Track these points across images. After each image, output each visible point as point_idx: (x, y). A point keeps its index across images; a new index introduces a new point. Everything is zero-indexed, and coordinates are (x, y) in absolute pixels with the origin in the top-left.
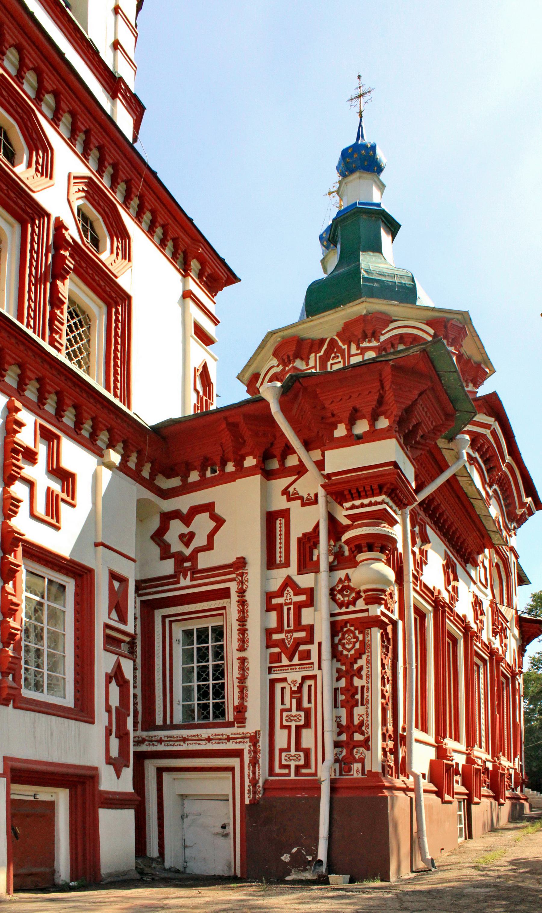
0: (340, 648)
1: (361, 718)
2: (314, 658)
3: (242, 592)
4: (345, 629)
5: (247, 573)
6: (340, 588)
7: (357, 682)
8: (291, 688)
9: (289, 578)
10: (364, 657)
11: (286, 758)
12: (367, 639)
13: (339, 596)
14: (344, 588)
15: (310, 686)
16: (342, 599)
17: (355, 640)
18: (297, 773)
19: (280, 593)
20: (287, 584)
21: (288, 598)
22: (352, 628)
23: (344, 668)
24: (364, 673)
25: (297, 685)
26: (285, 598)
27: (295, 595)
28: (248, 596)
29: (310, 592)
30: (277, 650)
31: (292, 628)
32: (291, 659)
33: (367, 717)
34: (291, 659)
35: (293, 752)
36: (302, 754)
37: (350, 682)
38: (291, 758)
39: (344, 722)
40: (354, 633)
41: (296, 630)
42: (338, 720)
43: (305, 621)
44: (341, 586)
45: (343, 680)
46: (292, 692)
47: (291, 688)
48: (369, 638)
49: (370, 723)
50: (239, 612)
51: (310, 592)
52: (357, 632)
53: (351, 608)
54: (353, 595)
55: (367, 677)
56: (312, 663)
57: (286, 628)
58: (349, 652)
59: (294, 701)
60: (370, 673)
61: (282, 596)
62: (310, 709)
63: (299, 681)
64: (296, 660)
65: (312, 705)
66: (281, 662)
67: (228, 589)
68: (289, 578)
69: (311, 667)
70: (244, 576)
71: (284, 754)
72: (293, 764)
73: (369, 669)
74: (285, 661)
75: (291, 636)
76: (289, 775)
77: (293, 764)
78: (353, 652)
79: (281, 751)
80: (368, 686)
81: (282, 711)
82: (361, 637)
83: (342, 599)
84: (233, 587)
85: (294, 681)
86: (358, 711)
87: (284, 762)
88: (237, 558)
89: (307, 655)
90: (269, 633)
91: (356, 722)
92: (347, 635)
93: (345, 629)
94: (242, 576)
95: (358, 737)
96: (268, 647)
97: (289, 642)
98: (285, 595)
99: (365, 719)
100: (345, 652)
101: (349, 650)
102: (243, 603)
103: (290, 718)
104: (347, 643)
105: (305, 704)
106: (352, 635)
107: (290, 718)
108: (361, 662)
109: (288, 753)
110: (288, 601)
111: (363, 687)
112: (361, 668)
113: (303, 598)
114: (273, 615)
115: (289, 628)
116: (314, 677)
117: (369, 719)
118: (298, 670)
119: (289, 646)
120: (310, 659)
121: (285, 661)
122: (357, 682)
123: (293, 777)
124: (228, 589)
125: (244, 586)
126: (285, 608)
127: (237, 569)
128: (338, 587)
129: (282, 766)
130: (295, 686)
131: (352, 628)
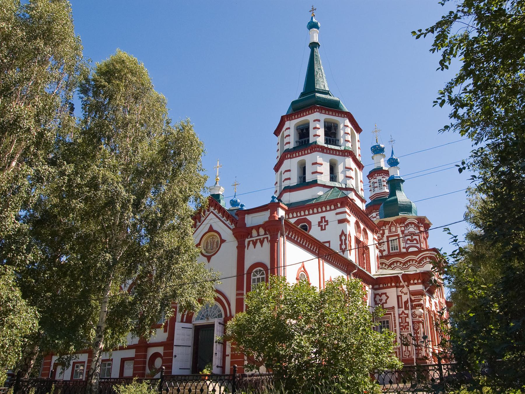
3: (394, 314)
29: (407, 314)
43: (407, 321)
51: (407, 314)
84: (392, 313)
89: (408, 329)
90: (400, 323)
102: (394, 316)
108: (419, 331)
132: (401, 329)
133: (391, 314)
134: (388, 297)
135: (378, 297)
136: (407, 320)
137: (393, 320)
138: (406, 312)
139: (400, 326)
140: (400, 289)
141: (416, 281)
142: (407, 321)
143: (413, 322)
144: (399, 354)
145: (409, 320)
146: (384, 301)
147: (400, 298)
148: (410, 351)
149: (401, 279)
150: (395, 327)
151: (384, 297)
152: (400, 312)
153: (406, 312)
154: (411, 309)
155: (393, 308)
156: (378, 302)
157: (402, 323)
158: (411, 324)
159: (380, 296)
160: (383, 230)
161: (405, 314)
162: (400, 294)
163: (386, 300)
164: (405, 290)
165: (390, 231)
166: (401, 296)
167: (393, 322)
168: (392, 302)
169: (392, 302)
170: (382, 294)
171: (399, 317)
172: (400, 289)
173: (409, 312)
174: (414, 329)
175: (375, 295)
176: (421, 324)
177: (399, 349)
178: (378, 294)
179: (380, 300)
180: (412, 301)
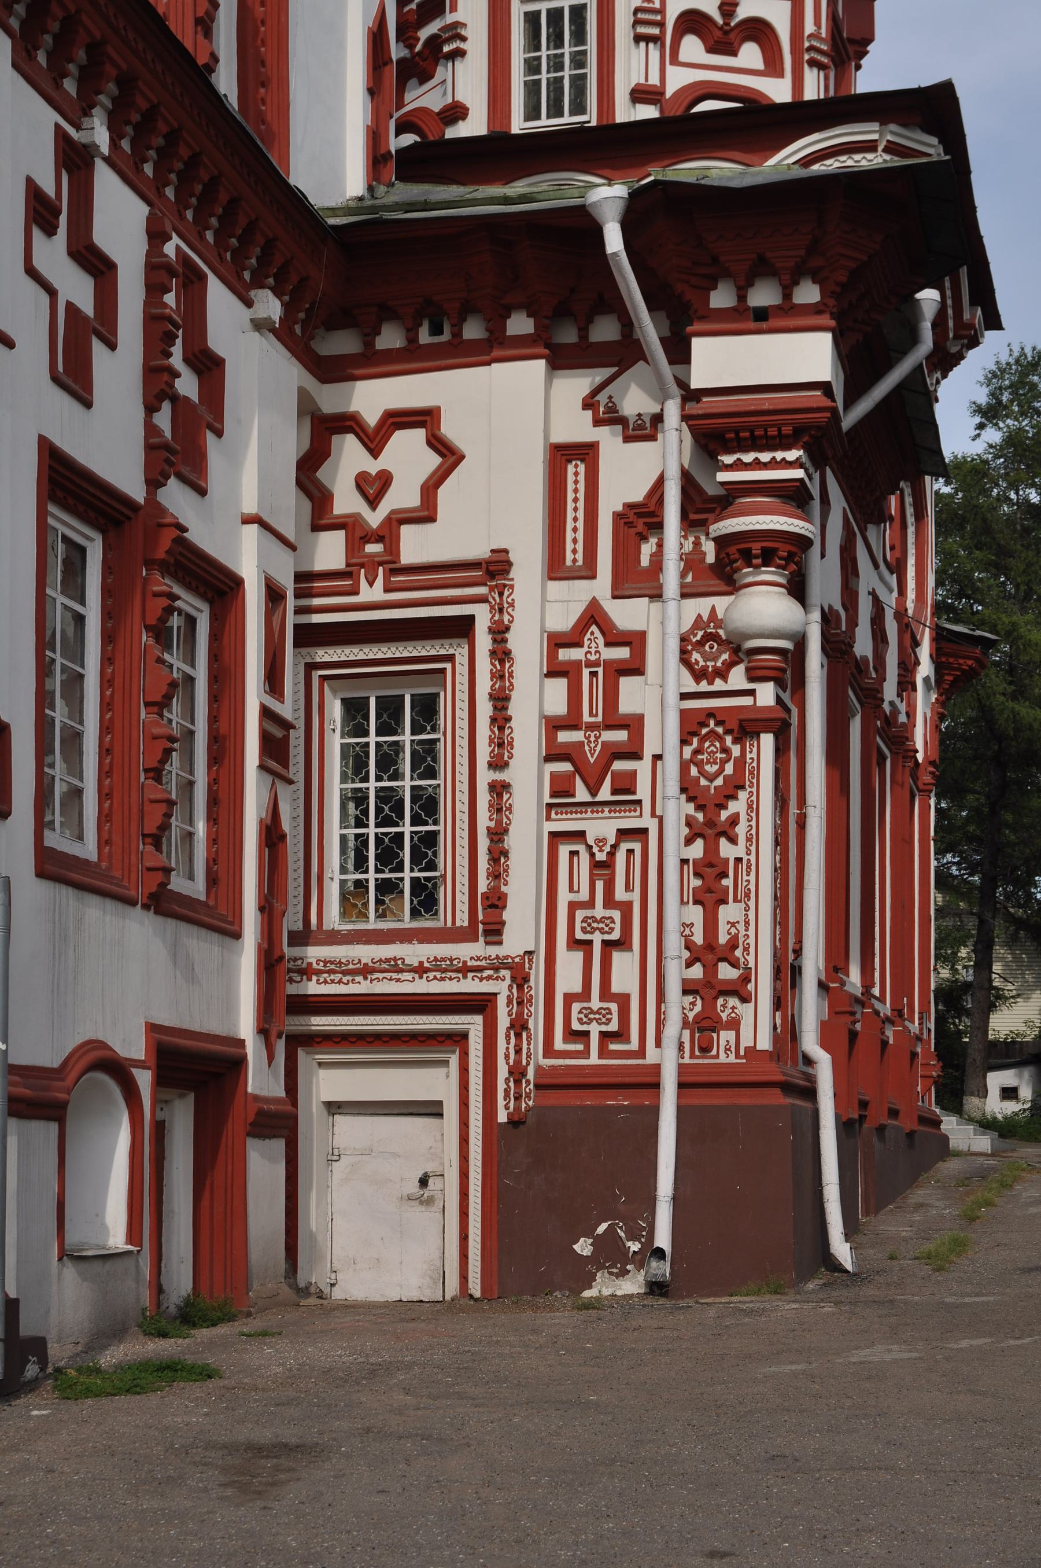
0: (694, 771)
1: (733, 931)
2: (643, 791)
3: (499, 632)
4: (704, 731)
5: (512, 587)
6: (698, 637)
7: (726, 850)
8: (592, 855)
9: (594, 604)
10: (742, 795)
11: (582, 1016)
12: (749, 756)
13: (696, 656)
14: (708, 637)
15: (630, 851)
16: (702, 663)
17: (724, 756)
18: (603, 1053)
19: (573, 639)
20: (592, 616)
21: (593, 650)
22: (720, 730)
23: (700, 816)
24: (741, 830)
25: (607, 849)
26: (586, 649)
27: (608, 644)
28: (514, 641)
29: (636, 641)
30: (566, 767)
31: (600, 718)
32: (594, 791)
33: (747, 930)
34: (594, 791)
35: (595, 1003)
36: (614, 1007)
37: (712, 849)
38: (591, 1016)
39: (698, 939)
40: (721, 740)
41: (609, 727)
42: (687, 932)
43: (626, 706)
44: (700, 633)
45: (699, 843)
46: (595, 865)
47: (592, 855)
48: (754, 755)
49: (752, 941)
50: (493, 676)
51: (636, 641)
52: (729, 739)
53: (719, 685)
54: (725, 656)
55: (749, 840)
56: (639, 802)
57: (586, 718)
58: (711, 781)
59: (600, 885)
60: (753, 832)
61: (579, 644)
62: (629, 904)
63: (612, 840)
64: (605, 793)
65: (635, 897)
66: (573, 795)
67: (471, 619)
68: (594, 604)
69: (635, 811)
70: (506, 593)
71: (576, 1007)
72: (595, 1029)
73: (754, 823)
74: (582, 794)
75: (597, 738)
76: (586, 1053)
77: (595, 1029)
78: (719, 781)
79: (570, 999)
80: (749, 860)
81: (573, 906)
82: (736, 751)
83: (702, 663)
85: (601, 841)
86: (729, 913)
87: (576, 1026)
88: (492, 551)
89: (625, 785)
90: (553, 725)
91: (723, 939)
92: (707, 744)
93: (704, 731)
94: (501, 594)
95: (726, 972)
96: (549, 758)
97: (592, 751)
98: (586, 643)
99: (743, 932)
100: (703, 782)
101: (711, 779)
102: (501, 654)
103: (589, 925)
104: (708, 762)
105: (620, 894)
106: (718, 744)
107: (589, 925)
108: (737, 806)
109: (585, 1005)
110: (593, 658)
111: (739, 860)
112: (734, 820)
113: (622, 653)
114: (559, 686)
115: (593, 720)
116: (641, 833)
117: (751, 932)
118: (606, 814)
119: (592, 760)
120: (634, 793)
121: (582, 794)
122: (726, 850)
123: (594, 1059)
124: (471, 619)
125: (506, 618)
126: (586, 672)
127: (492, 575)
128: (695, 635)
129: (572, 1035)
130: (601, 851)
131: (720, 730)
132: (561, 788)
134: (450, 456)
135: (350, 457)
136: (632, 696)
137: (484, 685)
138: (627, 614)
142: (626, 706)
143: (691, 726)
144: (519, 1026)
145: (656, 697)
146: (403, 495)
147: (575, 472)
148: (623, 1000)
149: (614, 240)
150: (498, 764)
151: (408, 456)
152: (563, 621)
153: (627, 614)
155: (495, 568)
156: (346, 501)
157: (571, 722)
158: (662, 735)
159: (374, 441)
162: (575, 426)
163: (430, 489)
167: (485, 710)
169: (493, 508)
170: (398, 419)
172: (576, 385)
173: (664, 621)
174: (688, 789)
175: (325, 429)
176: (767, 741)
179: (362, 482)
180: (700, 507)
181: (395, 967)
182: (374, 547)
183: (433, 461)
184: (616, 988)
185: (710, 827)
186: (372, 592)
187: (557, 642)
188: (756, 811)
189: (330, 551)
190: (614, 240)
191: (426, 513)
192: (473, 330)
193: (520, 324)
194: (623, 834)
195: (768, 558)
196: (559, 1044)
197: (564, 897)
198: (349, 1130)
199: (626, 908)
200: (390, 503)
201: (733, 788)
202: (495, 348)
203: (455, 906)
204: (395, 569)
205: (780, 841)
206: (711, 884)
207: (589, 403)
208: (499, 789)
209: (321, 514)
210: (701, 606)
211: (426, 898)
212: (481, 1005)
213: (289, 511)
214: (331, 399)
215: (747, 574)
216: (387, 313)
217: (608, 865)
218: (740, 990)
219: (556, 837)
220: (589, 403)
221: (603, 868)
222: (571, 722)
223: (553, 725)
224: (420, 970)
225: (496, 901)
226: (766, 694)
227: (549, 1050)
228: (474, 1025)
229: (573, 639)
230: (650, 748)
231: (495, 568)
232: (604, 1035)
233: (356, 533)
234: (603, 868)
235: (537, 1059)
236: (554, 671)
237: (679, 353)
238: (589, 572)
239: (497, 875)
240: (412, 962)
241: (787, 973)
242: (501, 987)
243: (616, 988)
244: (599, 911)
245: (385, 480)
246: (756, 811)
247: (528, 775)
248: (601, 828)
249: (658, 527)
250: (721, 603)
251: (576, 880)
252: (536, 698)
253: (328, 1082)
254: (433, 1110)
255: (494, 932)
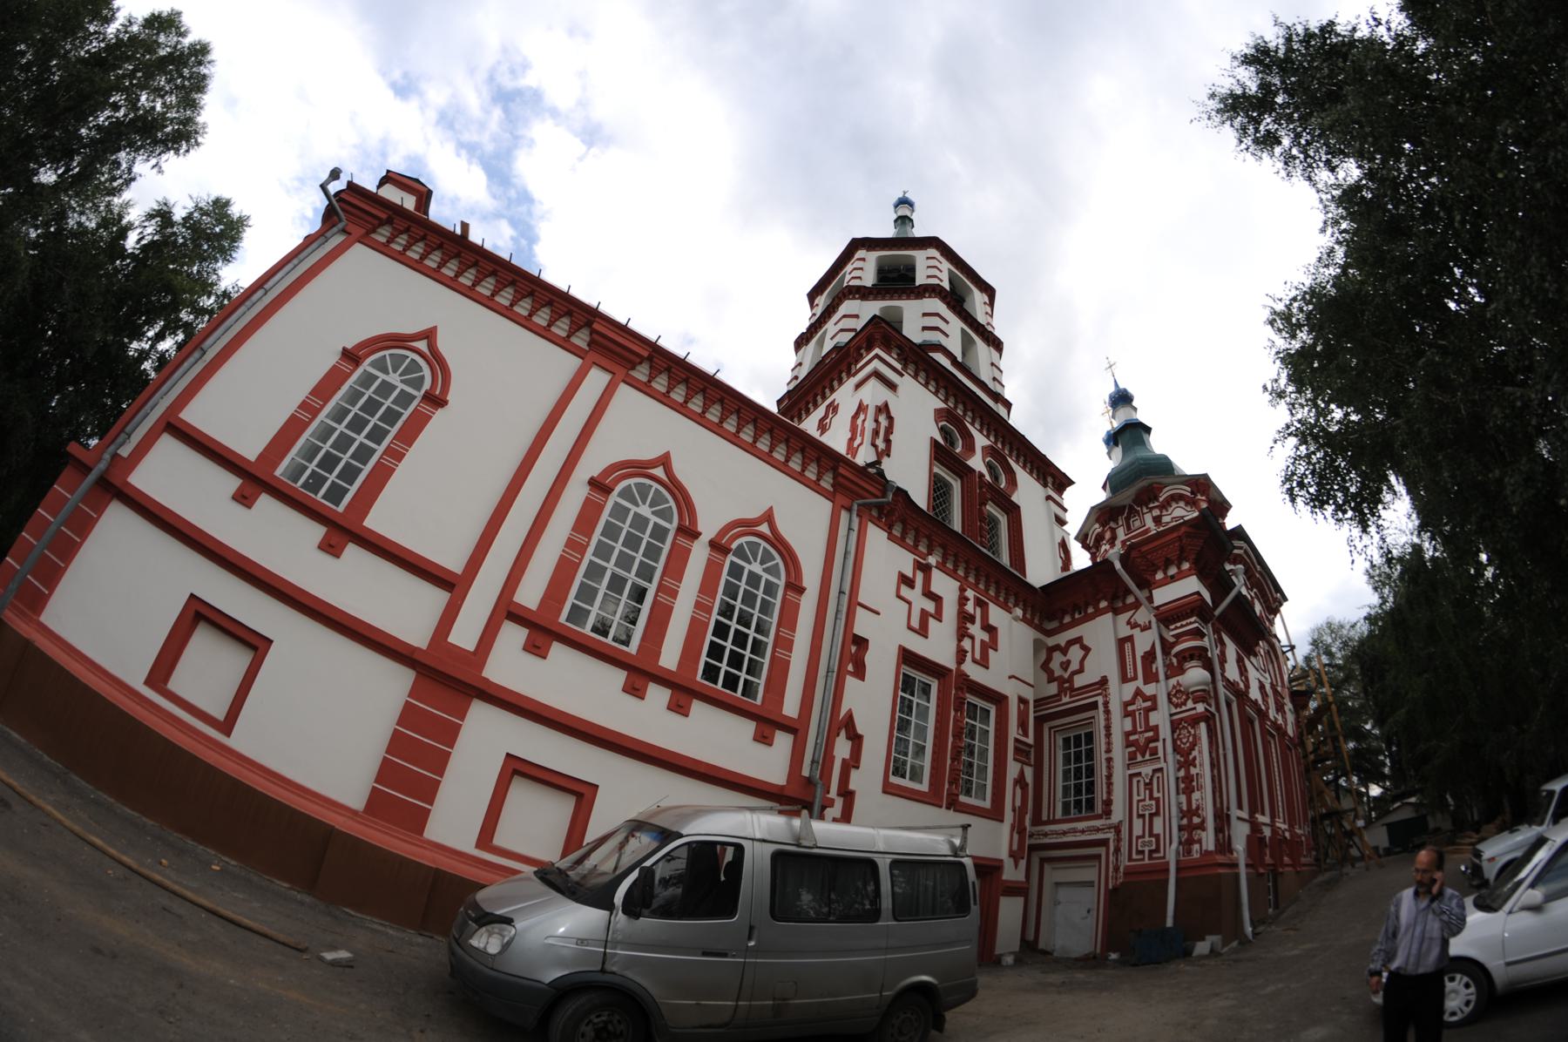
2: (1161, 754)
3: (1106, 704)
7: (1193, 771)
18: (1150, 858)
19: (1132, 702)
28: (1111, 707)
29: (1153, 698)
37: (1188, 771)
51: (1153, 698)
72: (1146, 849)
74: (1139, 758)
77: (1146, 849)
84: (1100, 700)
89: (1154, 752)
102: (1107, 712)
105: (1156, 795)
108: (1195, 753)
113: (1149, 704)
114: (1128, 720)
116: (1161, 770)
121: (1139, 758)
122: (1193, 771)
129: (1139, 852)
132: (1132, 757)
133: (1094, 706)
134: (1087, 650)
135: (1058, 658)
136: (1154, 718)
137: (1102, 723)
139: (1129, 744)
140: (1127, 615)
141: (1173, 571)
143: (1175, 726)
144: (1117, 850)
145: (1161, 718)
146: (1074, 666)
147: (1128, 646)
148: (1157, 837)
149: (1118, 566)
150: (1108, 751)
151: (1075, 653)
152: (1128, 697)
153: (1149, 690)
154: (1167, 678)
155: (1104, 682)
156: (1058, 672)
157: (1134, 732)
158: (1165, 732)
159: (1064, 651)
160: (1113, 531)
161: (1146, 699)
162: (1125, 631)
163: (1082, 662)
164: (1143, 615)
165: (1129, 528)
166: (1130, 639)
167: (1103, 732)
168: (1102, 662)
169: (1102, 662)
170: (1071, 643)
171: (1127, 714)
173: (1159, 689)
174: (1176, 749)
176: (1203, 726)
177: (1117, 829)
178: (1057, 648)
179: (1062, 664)
181: (1075, 831)
182: (1066, 685)
183: (1082, 653)
184: (1155, 831)
185: (1186, 762)
186: (1066, 699)
187: (1126, 704)
188: (1203, 753)
189: (1053, 689)
190: (1118, 566)
191: (1081, 670)
192: (1090, 610)
193: (1103, 604)
194: (1155, 771)
195: (1192, 658)
196: (1134, 856)
197: (1136, 798)
198: (1063, 893)
199: (1157, 800)
200: (1070, 670)
201: (1193, 745)
202: (1099, 612)
203: (1099, 809)
204: (1072, 689)
205: (1212, 766)
206: (1188, 785)
207: (1129, 623)
208: (1109, 760)
209: (1051, 679)
210: (1173, 681)
211: (1091, 804)
212: (1104, 843)
213: (1028, 670)
214: (1051, 642)
215: (1187, 665)
216: (1064, 612)
217: (1151, 783)
218: (1202, 826)
219: (1131, 776)
220: (1129, 623)
221: (1149, 785)
222: (1134, 732)
223: (1128, 734)
224: (1083, 832)
225: (1108, 803)
226: (1201, 708)
227: (1130, 859)
228: (1102, 851)
229: (1132, 702)
230: (1161, 737)
231: (1104, 682)
232: (1151, 852)
233: (1061, 681)
234: (1149, 785)
235: (1124, 862)
236: (1127, 714)
237: (1150, 599)
238: (1135, 678)
239: (1109, 792)
240: (1083, 828)
241: (1222, 819)
242: (1111, 835)
243: (1155, 831)
244: (1148, 802)
245: (1069, 662)
246: (1203, 753)
247: (1119, 753)
248: (1147, 770)
249: (1155, 658)
250: (1180, 678)
251: (1140, 794)
252: (1120, 725)
253: (1053, 875)
254: (1090, 884)
255: (1107, 813)
